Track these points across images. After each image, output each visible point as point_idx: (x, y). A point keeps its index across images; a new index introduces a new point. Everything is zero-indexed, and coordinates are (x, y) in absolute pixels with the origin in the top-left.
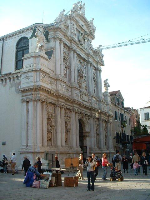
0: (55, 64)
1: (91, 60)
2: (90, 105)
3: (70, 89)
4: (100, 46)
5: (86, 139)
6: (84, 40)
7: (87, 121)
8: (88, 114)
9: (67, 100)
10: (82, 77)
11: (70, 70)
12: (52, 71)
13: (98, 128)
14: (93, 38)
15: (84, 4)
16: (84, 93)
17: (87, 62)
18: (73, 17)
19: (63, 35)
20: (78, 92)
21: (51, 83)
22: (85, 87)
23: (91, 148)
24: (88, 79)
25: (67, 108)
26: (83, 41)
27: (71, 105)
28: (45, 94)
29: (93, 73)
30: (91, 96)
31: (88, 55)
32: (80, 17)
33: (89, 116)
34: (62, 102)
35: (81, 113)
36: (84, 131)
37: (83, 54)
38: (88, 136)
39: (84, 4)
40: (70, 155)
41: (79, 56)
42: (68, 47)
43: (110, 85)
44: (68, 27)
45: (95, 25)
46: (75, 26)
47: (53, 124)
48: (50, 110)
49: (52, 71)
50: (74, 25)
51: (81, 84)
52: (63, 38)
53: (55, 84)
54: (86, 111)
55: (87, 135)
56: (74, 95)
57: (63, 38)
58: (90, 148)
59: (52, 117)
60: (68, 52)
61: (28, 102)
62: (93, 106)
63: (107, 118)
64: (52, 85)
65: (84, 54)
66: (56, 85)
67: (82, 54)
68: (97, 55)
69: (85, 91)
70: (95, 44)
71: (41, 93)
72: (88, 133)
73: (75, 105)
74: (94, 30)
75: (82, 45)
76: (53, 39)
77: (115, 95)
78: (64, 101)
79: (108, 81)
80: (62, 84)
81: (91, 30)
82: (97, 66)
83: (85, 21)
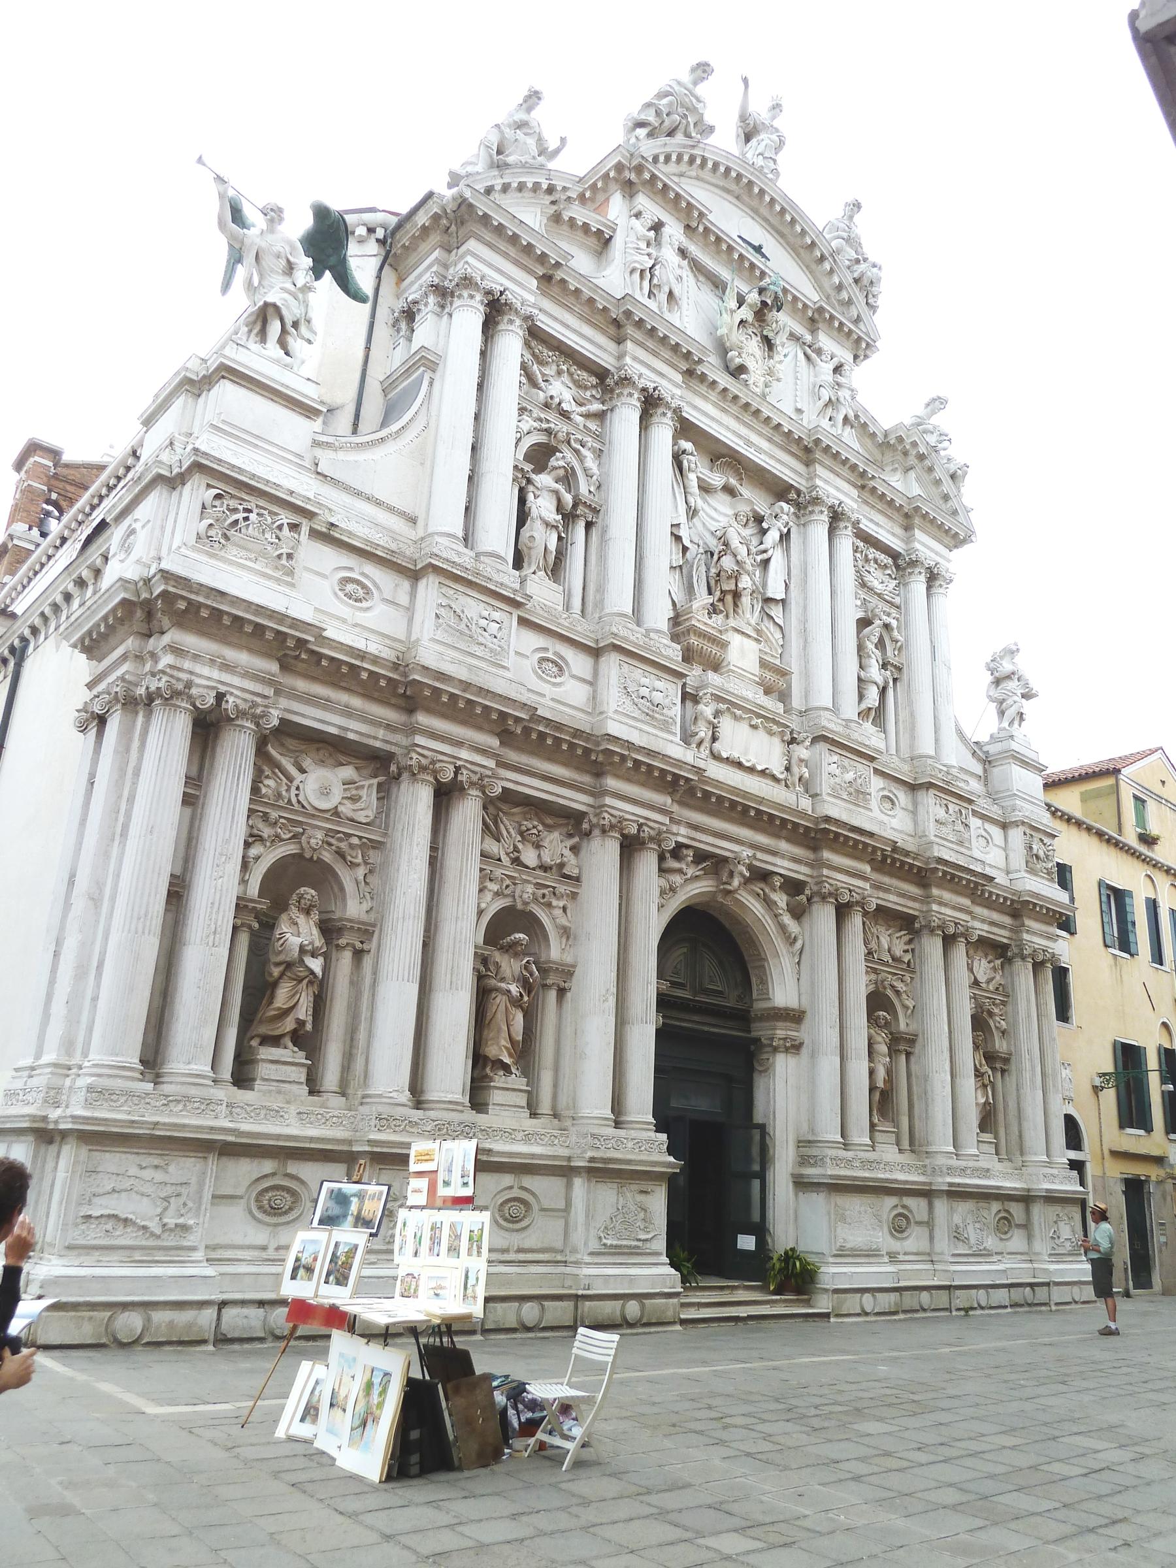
0: (425, 460)
1: (833, 488)
2: (805, 804)
3: (579, 663)
4: (937, 403)
5: (767, 1070)
6: (768, 343)
7: (783, 928)
8: (782, 866)
9: (518, 730)
10: (736, 595)
11: (604, 531)
12: (403, 514)
13: (900, 986)
14: (861, 347)
15: (776, 107)
16: (729, 705)
17: (798, 506)
18: (639, 169)
19: (530, 272)
20: (667, 692)
21: (350, 587)
22: (755, 668)
23: (806, 1146)
24: (805, 621)
25: (508, 796)
26: (753, 346)
27: (586, 779)
28: (243, 658)
29: (863, 585)
30: (824, 738)
31: (808, 451)
32: (733, 187)
33: (793, 887)
34: (459, 744)
35: (701, 857)
36: (759, 1005)
37: (754, 438)
38: (795, 1048)
39: (776, 107)
40: (528, 1181)
41: (721, 455)
42: (601, 374)
43: (1035, 685)
44: (603, 242)
45: (871, 251)
46: (674, 231)
47: (354, 909)
48: (325, 792)
49: (403, 514)
50: (657, 227)
51: (724, 645)
52: (522, 290)
53: (404, 599)
54: (754, 846)
55: (781, 1031)
56: (613, 699)
57: (522, 290)
58: (803, 1143)
59: (340, 854)
60: (596, 407)
61: (102, 720)
62: (836, 809)
63: (1007, 920)
64: (364, 604)
65: (770, 440)
66: (410, 610)
67: (749, 443)
68: (907, 470)
69: (754, 695)
70: (885, 391)
71: (191, 641)
72: (795, 1017)
73: (611, 783)
74: (866, 286)
75: (742, 369)
76: (432, 299)
77: (1117, 771)
78: (494, 742)
79: (1023, 664)
80: (473, 607)
81: (840, 288)
82: (908, 540)
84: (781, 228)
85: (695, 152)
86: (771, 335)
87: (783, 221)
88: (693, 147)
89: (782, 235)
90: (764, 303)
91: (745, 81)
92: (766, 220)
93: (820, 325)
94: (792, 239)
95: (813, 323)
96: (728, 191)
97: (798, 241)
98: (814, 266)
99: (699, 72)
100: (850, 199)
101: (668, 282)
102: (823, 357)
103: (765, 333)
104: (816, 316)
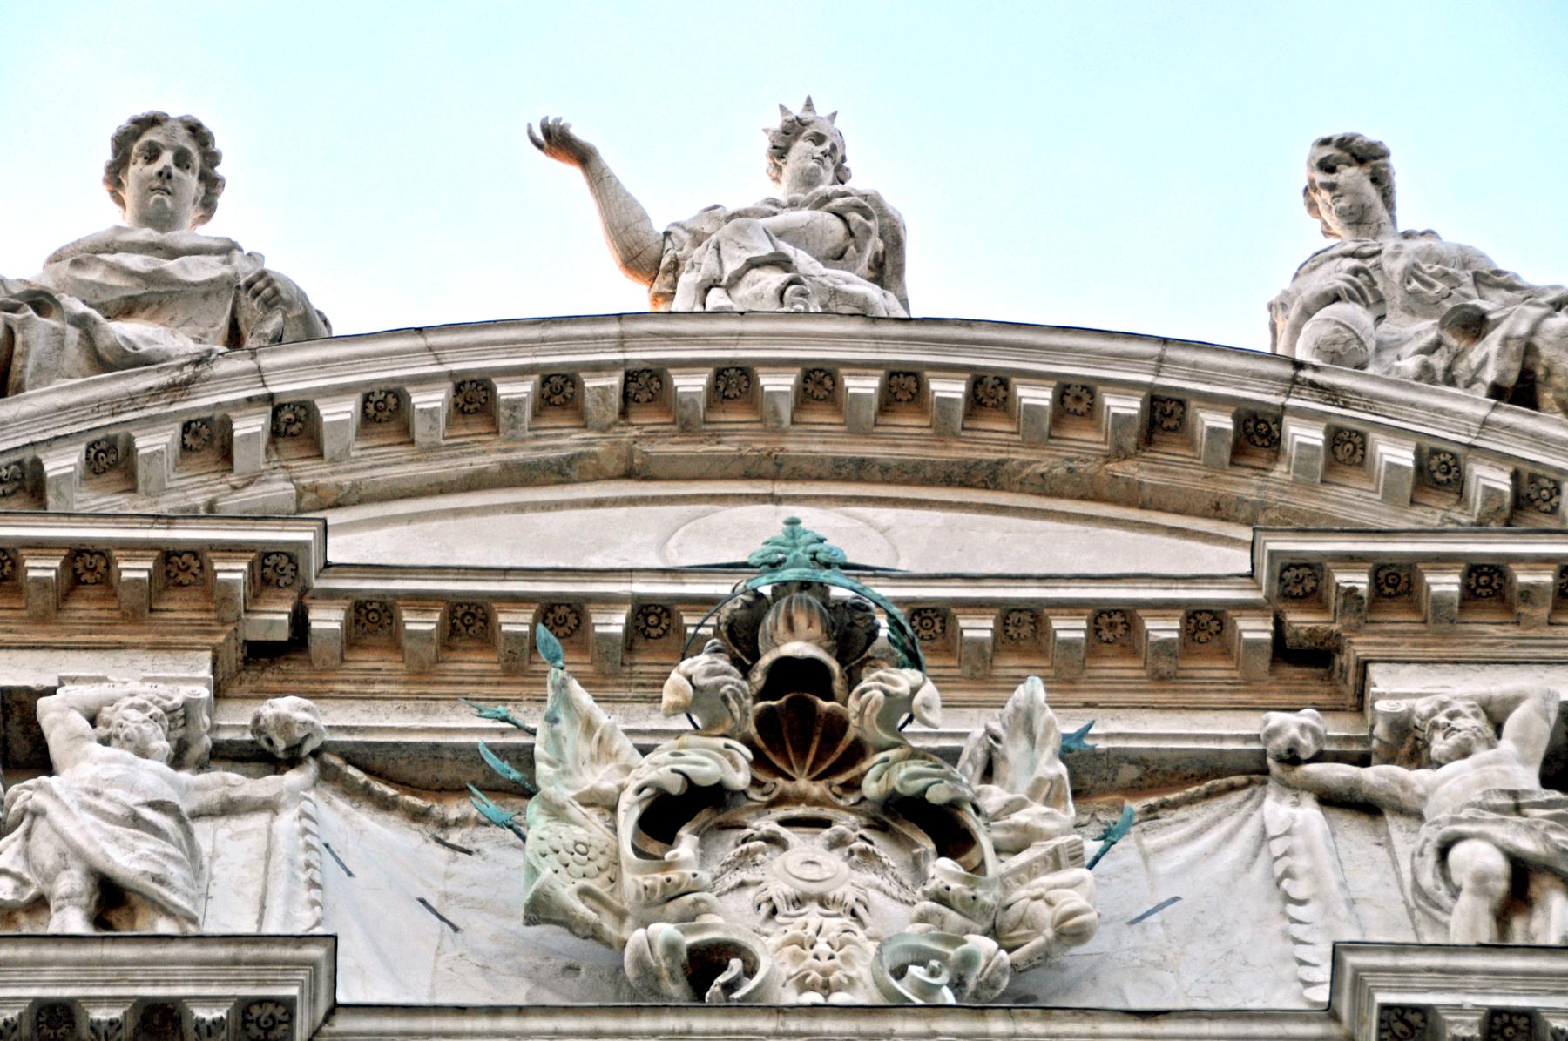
32: (567, 440)
83: (1142, 426)
84: (958, 452)
85: (202, 401)
86: (905, 776)
87: (943, 424)
88: (179, 389)
89: (990, 476)
90: (795, 677)
91: (557, 142)
92: (858, 470)
93: (1359, 647)
94: (1045, 461)
95: (1307, 660)
96: (560, 472)
97: (1089, 439)
98: (1245, 486)
99: (137, 170)
100: (1301, 173)
101: (72, 852)
102: (1439, 745)
103: (871, 788)
104: (1300, 620)
